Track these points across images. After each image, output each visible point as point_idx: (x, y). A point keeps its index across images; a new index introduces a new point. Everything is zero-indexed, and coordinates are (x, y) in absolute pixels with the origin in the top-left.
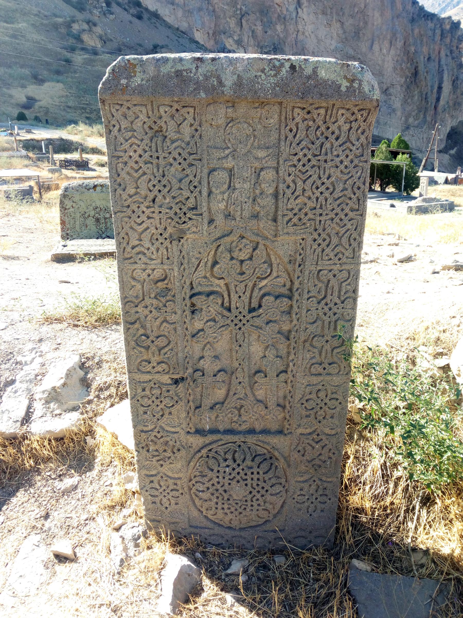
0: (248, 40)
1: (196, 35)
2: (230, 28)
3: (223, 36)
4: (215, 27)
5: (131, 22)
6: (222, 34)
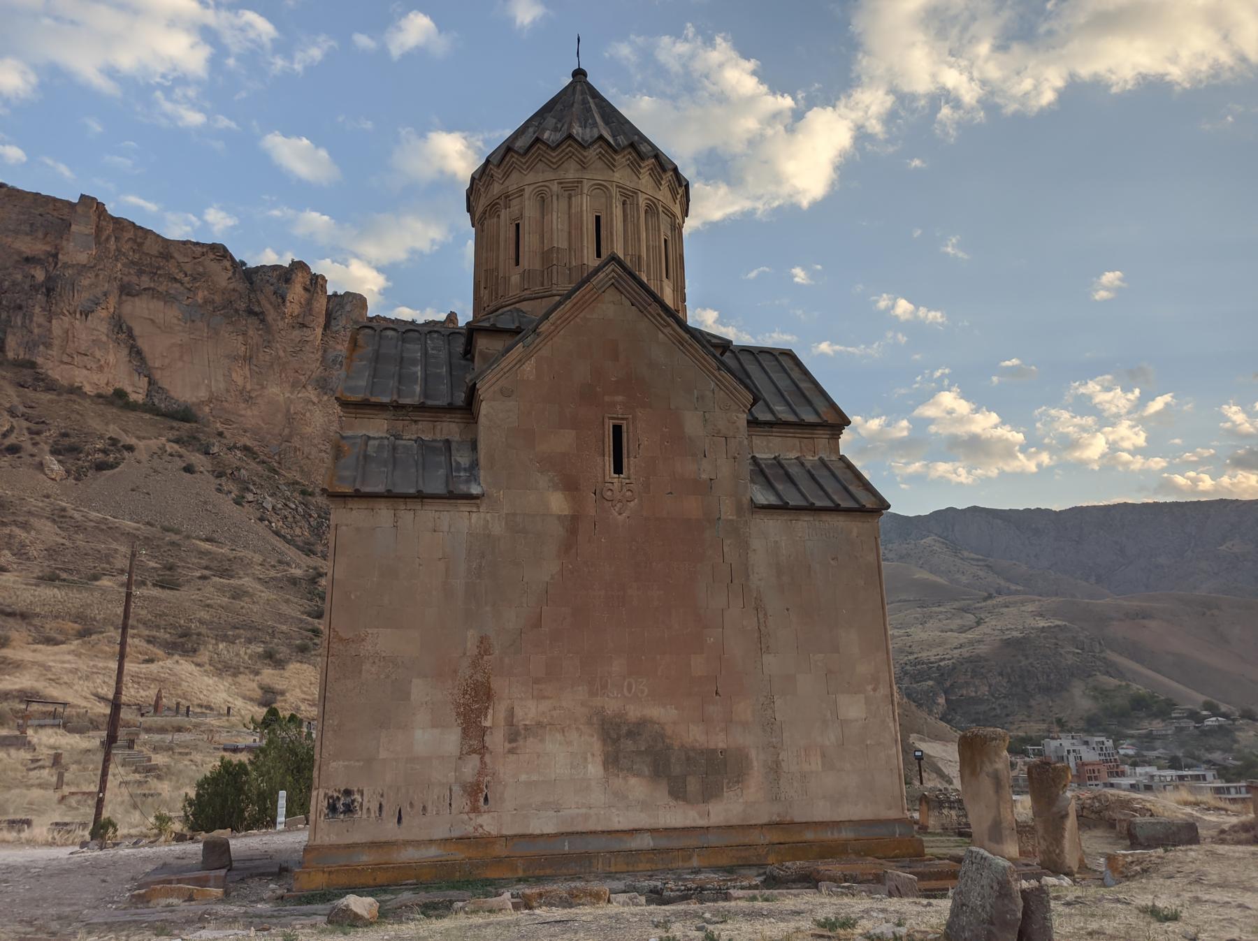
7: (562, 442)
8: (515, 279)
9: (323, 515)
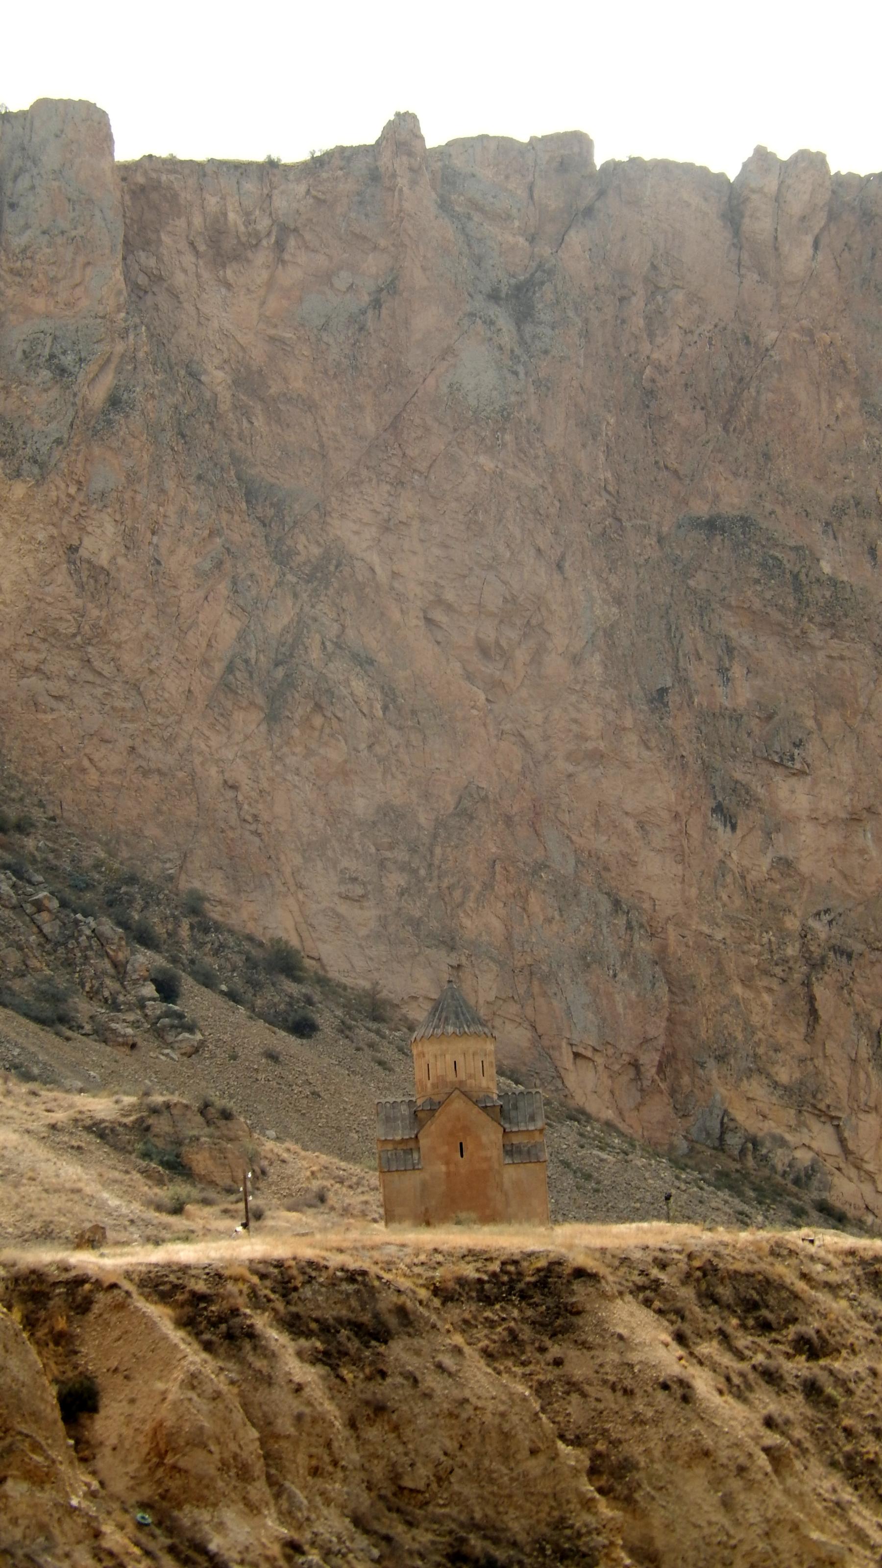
0: (853, 1081)
1: (571, 1080)
2: (749, 1029)
3: (713, 1070)
4: (670, 1032)
5: (272, 1057)
6: (711, 1064)
7: (444, 1149)
8: (429, 1085)
9: (69, 894)
